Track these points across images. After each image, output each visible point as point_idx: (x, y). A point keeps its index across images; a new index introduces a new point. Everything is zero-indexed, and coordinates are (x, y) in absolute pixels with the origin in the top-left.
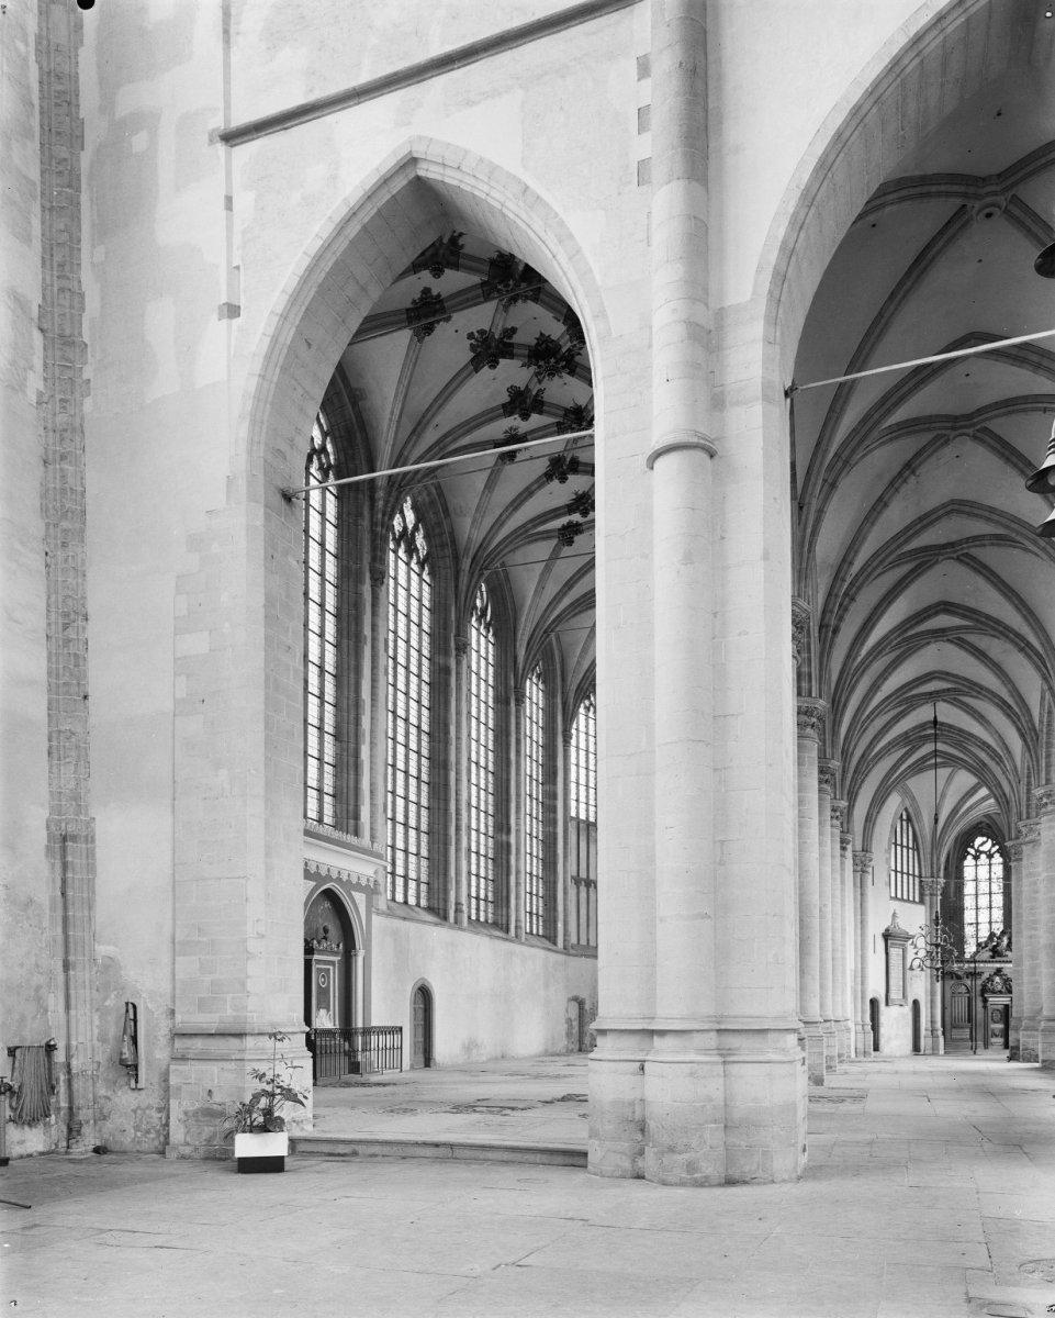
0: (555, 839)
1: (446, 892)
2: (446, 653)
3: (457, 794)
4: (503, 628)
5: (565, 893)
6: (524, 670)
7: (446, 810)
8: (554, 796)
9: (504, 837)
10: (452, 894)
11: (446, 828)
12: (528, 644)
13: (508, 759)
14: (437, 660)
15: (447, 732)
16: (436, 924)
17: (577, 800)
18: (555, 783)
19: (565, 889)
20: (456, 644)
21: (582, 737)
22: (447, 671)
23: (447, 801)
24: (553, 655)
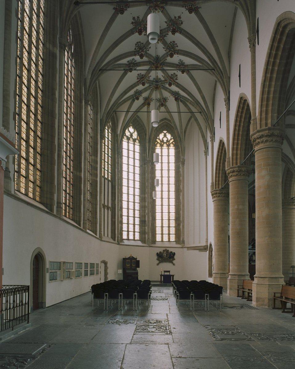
0: (97, 183)
1: (52, 194)
2: (54, 45)
3: (58, 135)
4: (79, 59)
5: (100, 211)
6: (89, 87)
7: (53, 142)
8: (96, 162)
9: (78, 174)
10: (56, 196)
11: (52, 153)
12: (92, 75)
13: (81, 131)
14: (48, 45)
15: (54, 94)
16: (47, 212)
17: (104, 168)
18: (97, 157)
19: (100, 208)
20: (60, 43)
21: (106, 139)
22: (54, 56)
23: (53, 137)
24: (97, 95)
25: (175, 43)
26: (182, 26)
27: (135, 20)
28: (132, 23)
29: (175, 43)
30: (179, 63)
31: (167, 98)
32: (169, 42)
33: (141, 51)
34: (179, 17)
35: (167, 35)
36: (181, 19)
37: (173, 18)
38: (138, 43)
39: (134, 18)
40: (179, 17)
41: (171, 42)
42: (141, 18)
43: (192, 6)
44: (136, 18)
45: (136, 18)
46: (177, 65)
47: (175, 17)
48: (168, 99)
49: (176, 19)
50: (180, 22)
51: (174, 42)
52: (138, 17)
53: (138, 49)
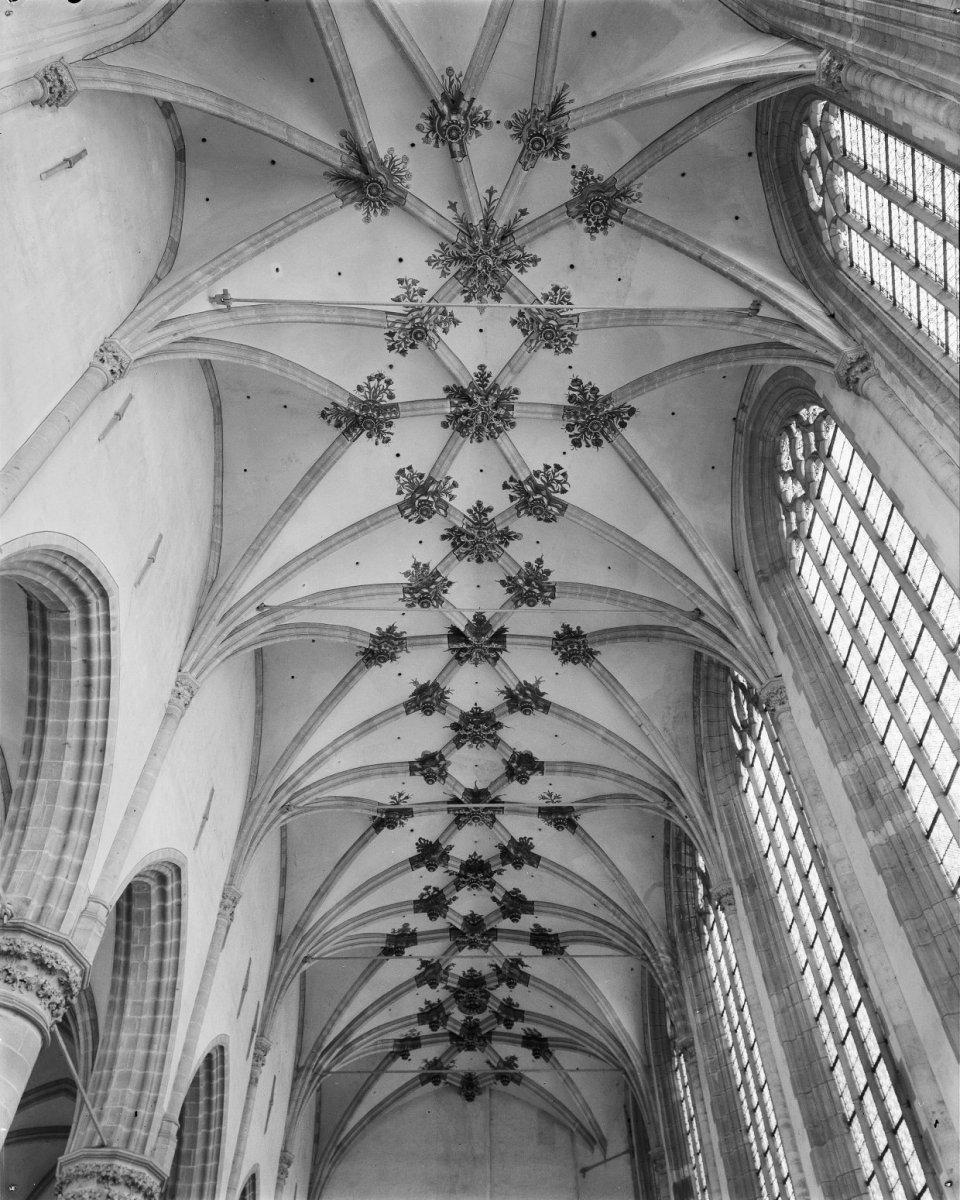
31: (426, 140)
48: (419, 128)
51: (420, 521)
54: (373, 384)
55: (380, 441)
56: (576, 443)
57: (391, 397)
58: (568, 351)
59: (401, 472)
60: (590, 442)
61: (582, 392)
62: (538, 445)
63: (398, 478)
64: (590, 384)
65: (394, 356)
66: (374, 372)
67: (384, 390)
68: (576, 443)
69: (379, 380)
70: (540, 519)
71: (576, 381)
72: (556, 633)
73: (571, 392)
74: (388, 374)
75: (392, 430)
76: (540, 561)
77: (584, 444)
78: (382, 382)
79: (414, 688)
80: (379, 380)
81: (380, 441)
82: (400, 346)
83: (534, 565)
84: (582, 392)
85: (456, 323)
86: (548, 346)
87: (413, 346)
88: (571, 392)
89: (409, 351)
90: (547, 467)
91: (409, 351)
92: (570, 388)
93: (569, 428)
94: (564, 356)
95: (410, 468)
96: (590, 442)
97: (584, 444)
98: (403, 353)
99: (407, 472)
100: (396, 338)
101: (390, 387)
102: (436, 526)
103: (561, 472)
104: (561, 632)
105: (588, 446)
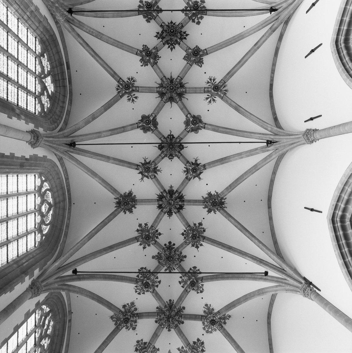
25: (197, 269)
26: (205, 234)
27: (142, 227)
28: (138, 230)
29: (197, 269)
30: (205, 311)
32: (189, 269)
33: (146, 279)
34: (200, 224)
35: (184, 259)
36: (203, 227)
37: (192, 225)
38: (142, 268)
39: (140, 225)
40: (200, 224)
41: (191, 269)
42: (149, 225)
43: (215, 200)
44: (143, 225)
45: (143, 225)
46: (202, 316)
47: (195, 224)
49: (196, 227)
50: (202, 230)
51: (195, 267)
52: (146, 224)
53: (142, 278)
54: (210, 330)
55: (209, 305)
56: (133, 303)
57: (204, 323)
58: (138, 342)
59: (201, 292)
60: (127, 306)
61: (131, 325)
62: (147, 302)
63: (203, 290)
64: (129, 330)
65: (202, 339)
66: (210, 335)
67: (206, 326)
68: (133, 303)
69: (208, 330)
70: (145, 268)
71: (134, 329)
72: (135, 208)
73: (136, 324)
74: (204, 332)
75: (204, 309)
76: (144, 248)
77: (130, 304)
78: (207, 330)
79: (201, 176)
80: (208, 330)
81: (209, 305)
82: (200, 343)
83: (147, 246)
84: (131, 325)
85: (179, 349)
86: (145, 343)
87: (194, 343)
88: (136, 324)
89: (196, 341)
90: (144, 293)
91: (196, 341)
92: (136, 325)
93: (136, 309)
94: (140, 340)
95: (198, 293)
96: (127, 306)
97: (130, 304)
98: (198, 340)
99: (199, 291)
100: (201, 348)
101: (204, 326)
102: (187, 265)
103: (138, 292)
104: (133, 208)
105: (128, 304)
